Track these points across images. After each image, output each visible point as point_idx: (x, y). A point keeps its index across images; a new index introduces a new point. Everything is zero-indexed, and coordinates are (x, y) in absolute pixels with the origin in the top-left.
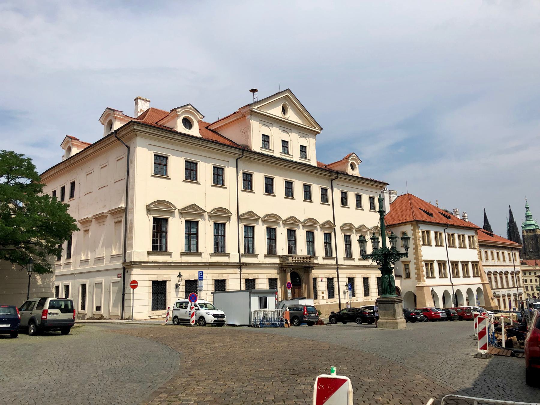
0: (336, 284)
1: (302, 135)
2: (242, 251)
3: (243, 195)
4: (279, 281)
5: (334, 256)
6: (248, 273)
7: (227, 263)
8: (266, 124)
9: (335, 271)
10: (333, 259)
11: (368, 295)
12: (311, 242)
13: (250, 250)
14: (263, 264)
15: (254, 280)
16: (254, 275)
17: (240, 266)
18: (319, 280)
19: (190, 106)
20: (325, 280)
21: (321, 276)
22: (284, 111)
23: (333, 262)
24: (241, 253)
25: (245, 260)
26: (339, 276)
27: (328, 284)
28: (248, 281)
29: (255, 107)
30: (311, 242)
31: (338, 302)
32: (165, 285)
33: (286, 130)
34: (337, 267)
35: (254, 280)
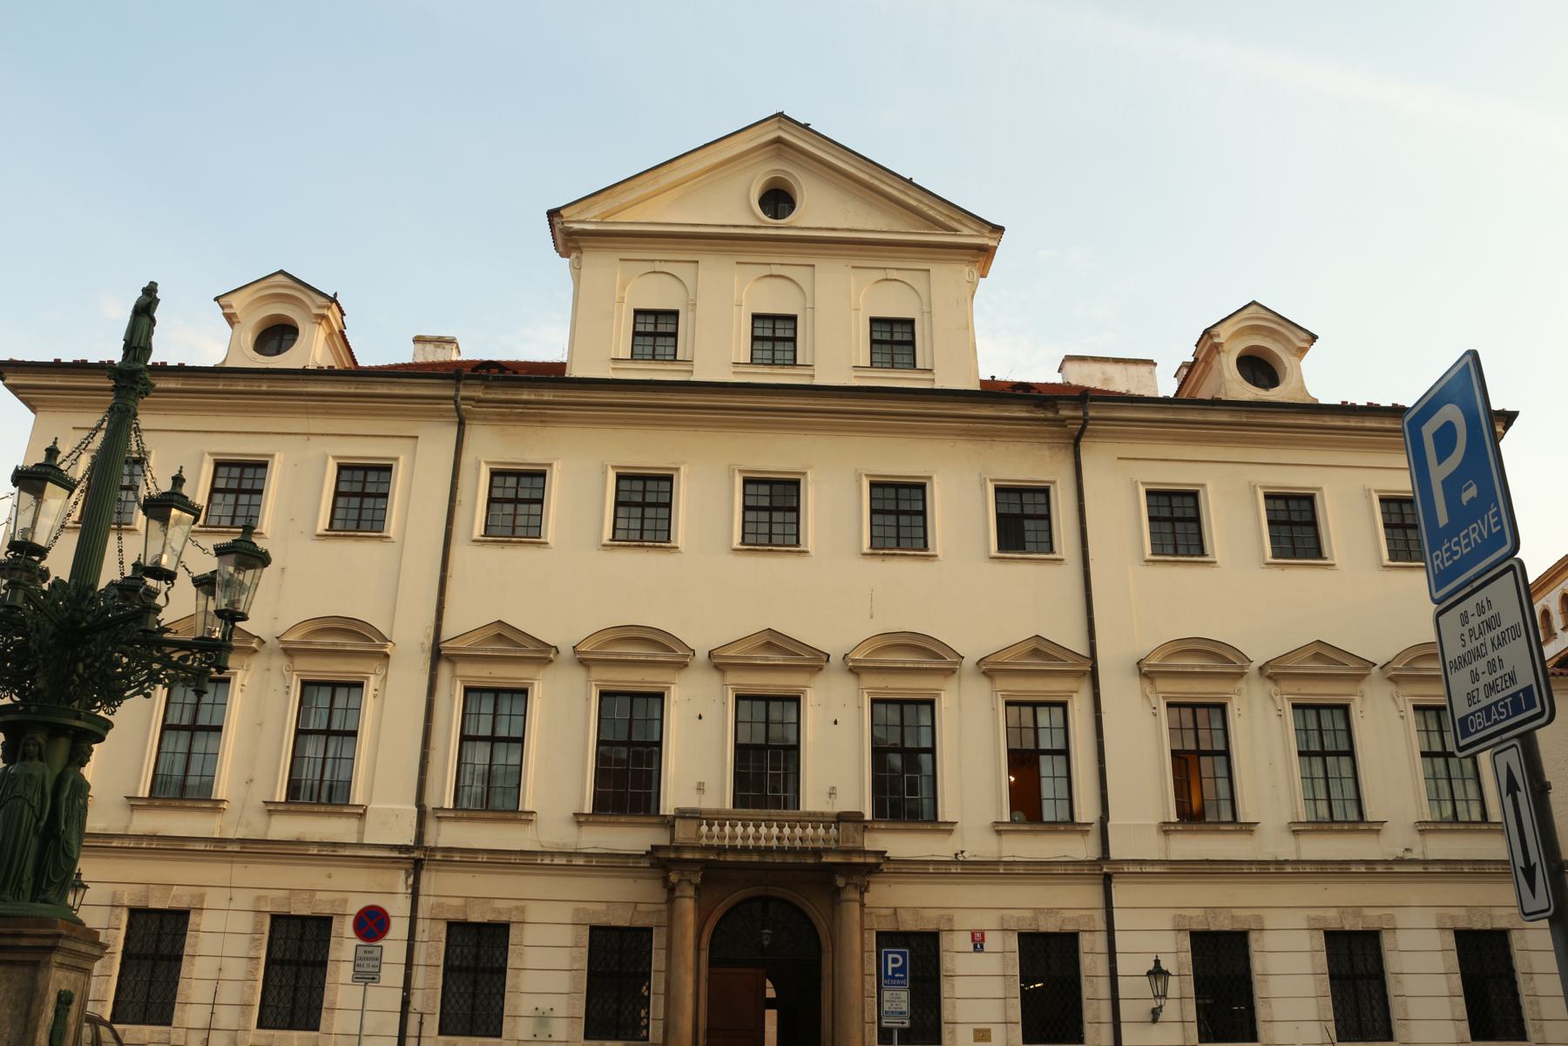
0: (1092, 962)
1: (881, 275)
2: (443, 794)
3: (472, 560)
4: (658, 941)
5: (1086, 811)
6: (451, 892)
8: (659, 267)
13: (493, 794)
14: (552, 854)
15: (505, 927)
16: (499, 904)
17: (416, 859)
19: (280, 278)
23: (1082, 849)
24: (431, 802)
25: (447, 835)
26: (1117, 925)
28: (457, 929)
33: (776, 270)
34: (1104, 872)
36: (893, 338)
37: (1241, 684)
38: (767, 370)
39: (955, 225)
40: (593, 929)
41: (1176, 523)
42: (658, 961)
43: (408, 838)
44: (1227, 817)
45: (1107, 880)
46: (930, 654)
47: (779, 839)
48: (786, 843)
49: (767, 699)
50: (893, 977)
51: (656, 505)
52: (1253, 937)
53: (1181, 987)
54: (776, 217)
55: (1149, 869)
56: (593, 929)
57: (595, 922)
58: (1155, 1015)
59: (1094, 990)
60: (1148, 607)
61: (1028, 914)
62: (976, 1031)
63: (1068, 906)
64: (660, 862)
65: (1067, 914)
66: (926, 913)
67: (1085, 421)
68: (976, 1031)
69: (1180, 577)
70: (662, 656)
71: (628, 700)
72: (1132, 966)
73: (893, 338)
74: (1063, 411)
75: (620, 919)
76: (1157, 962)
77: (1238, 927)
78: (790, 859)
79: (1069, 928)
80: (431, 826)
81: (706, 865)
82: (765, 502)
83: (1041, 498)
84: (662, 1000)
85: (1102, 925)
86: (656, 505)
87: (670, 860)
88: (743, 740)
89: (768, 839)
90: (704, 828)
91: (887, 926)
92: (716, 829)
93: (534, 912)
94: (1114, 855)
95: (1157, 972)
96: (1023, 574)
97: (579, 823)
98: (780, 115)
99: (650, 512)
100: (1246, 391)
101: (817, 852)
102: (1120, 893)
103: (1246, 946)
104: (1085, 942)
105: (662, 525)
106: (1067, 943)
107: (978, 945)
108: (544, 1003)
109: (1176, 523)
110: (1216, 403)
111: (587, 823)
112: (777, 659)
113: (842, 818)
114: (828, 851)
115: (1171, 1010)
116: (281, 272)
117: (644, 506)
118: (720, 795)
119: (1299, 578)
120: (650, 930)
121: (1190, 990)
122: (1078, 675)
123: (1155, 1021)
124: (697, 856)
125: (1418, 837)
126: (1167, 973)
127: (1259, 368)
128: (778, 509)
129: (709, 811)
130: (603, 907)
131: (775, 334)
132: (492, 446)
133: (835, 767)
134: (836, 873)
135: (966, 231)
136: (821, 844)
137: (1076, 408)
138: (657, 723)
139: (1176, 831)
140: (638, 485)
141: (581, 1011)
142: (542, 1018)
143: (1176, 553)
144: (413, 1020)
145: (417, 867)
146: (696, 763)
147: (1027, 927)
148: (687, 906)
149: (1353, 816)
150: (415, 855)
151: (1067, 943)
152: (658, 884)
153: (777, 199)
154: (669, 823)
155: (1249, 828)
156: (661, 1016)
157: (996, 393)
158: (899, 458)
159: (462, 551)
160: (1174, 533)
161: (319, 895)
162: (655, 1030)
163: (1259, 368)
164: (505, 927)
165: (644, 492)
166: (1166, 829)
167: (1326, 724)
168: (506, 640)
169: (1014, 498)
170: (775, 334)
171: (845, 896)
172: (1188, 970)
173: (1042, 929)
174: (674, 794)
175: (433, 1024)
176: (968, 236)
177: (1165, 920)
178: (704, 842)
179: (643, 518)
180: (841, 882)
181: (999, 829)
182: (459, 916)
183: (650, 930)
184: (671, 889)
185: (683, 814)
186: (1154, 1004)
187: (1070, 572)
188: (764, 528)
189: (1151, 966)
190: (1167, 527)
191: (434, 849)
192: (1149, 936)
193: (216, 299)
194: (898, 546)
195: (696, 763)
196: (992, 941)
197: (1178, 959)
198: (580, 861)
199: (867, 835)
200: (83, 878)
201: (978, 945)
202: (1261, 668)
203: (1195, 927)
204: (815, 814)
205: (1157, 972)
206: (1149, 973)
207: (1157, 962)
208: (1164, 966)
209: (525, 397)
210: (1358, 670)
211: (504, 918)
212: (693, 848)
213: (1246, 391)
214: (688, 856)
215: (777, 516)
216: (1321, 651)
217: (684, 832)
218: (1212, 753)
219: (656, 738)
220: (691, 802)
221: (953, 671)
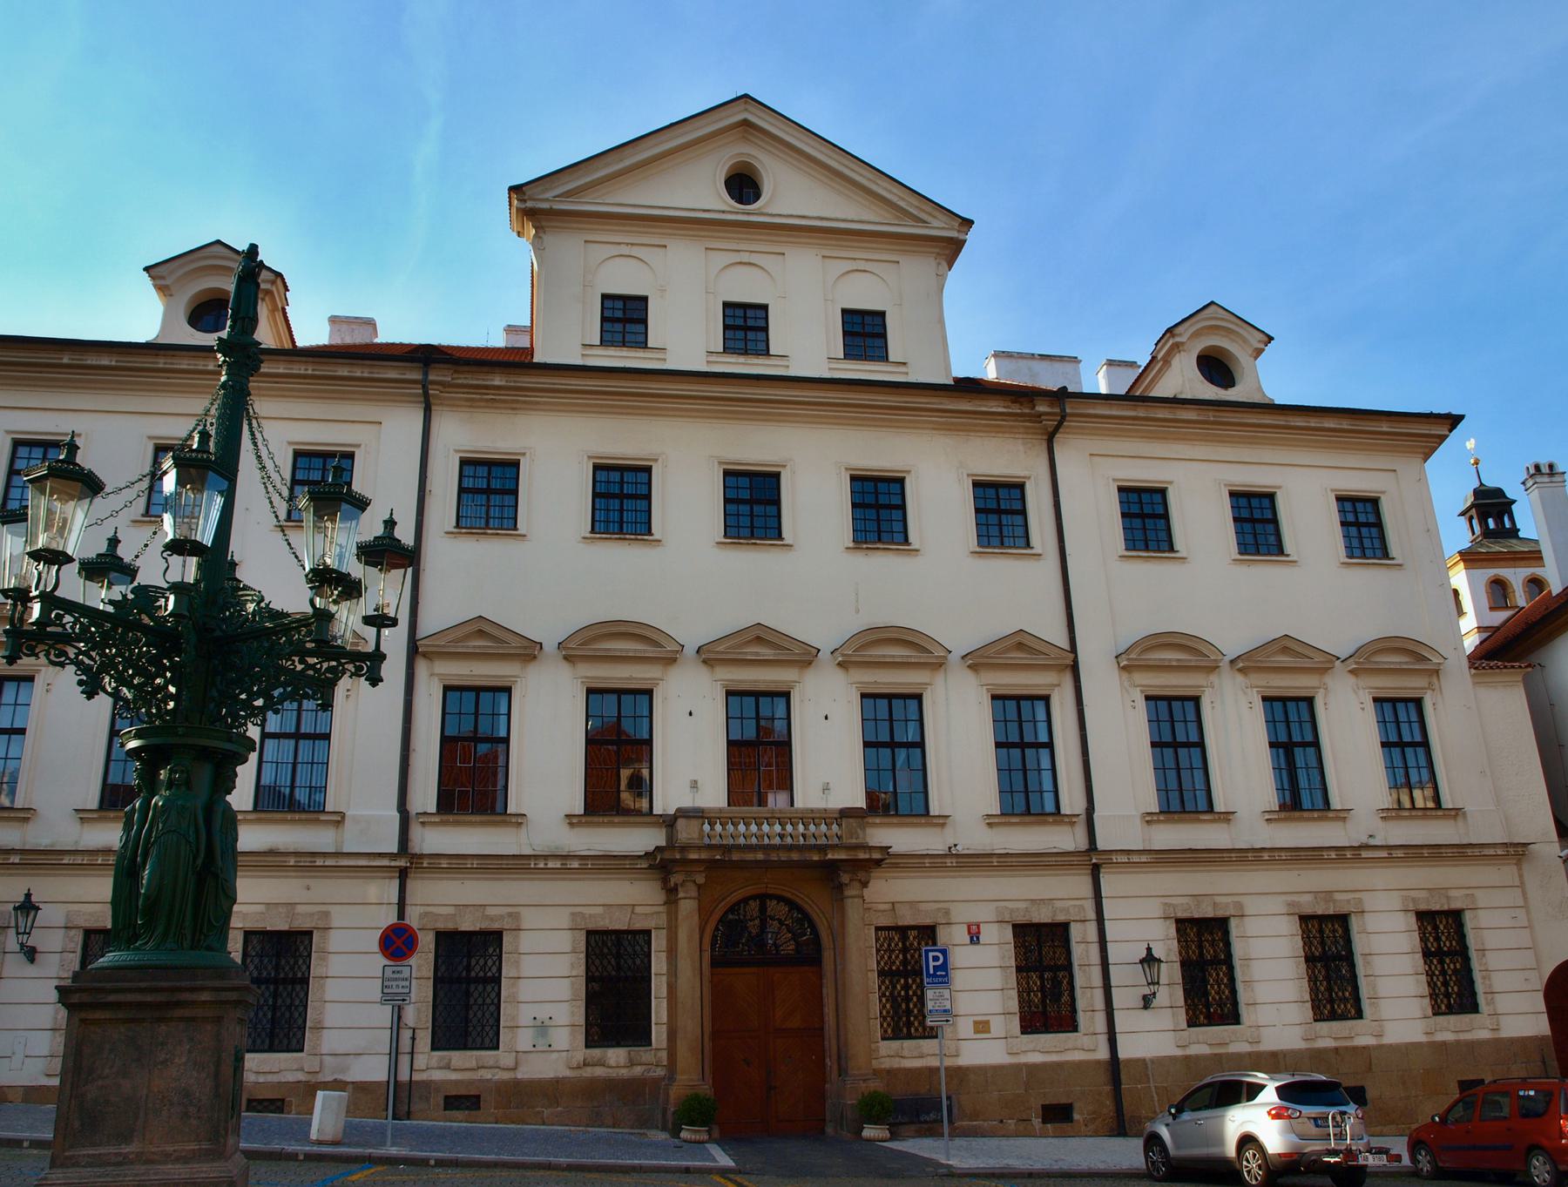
0: (1083, 951)
4: (658, 943)
5: (1072, 800)
6: (442, 902)
7: (325, 855)
8: (625, 250)
9: (1082, 884)
10: (1070, 820)
14: (546, 857)
15: (498, 935)
16: (491, 911)
21: (963, 914)
22: (743, 185)
23: (1068, 839)
25: (434, 840)
29: (549, 195)
31: (1103, 1054)
33: (745, 257)
35: (493, 939)
36: (864, 331)
37: (1213, 678)
38: (742, 359)
39: (928, 218)
40: (590, 933)
41: (1146, 519)
42: (658, 964)
44: (1202, 805)
45: (1095, 871)
46: (916, 648)
47: (782, 836)
48: (789, 840)
49: (757, 695)
50: (934, 975)
51: (635, 497)
52: (1233, 923)
53: (1170, 972)
54: (741, 202)
55: (1135, 858)
56: (590, 933)
57: (591, 926)
58: (1147, 1002)
59: (1086, 979)
60: (1122, 599)
61: (1022, 905)
62: (975, 1023)
63: (1062, 895)
64: (661, 865)
65: (1058, 904)
66: (923, 906)
67: (1063, 418)
68: (975, 1023)
69: (1149, 572)
70: (650, 651)
71: (614, 697)
72: (1125, 951)
73: (864, 331)
74: (1038, 407)
75: (619, 922)
76: (1149, 949)
77: (1220, 913)
78: (795, 856)
79: (1061, 918)
80: (416, 832)
81: (711, 865)
82: (746, 495)
83: (1016, 493)
84: (664, 1004)
85: (1092, 915)
86: (635, 497)
87: (675, 861)
88: (736, 736)
89: (782, 836)
90: (707, 827)
91: (884, 921)
92: (718, 827)
93: (529, 918)
94: (1101, 845)
95: (1149, 960)
96: (1004, 569)
97: (571, 825)
98: (746, 96)
99: (628, 504)
100: (1211, 392)
101: (822, 849)
102: (1108, 882)
103: (1226, 933)
104: (1075, 932)
105: (642, 517)
106: (1059, 932)
107: (975, 938)
108: (543, 1012)
109: (1146, 519)
110: (1175, 401)
111: (580, 824)
112: (766, 653)
113: (846, 813)
114: (834, 847)
115: (1163, 996)
117: (622, 500)
118: (714, 794)
119: (1263, 573)
120: (648, 933)
121: (1178, 977)
122: (1060, 668)
123: (1146, 1007)
124: (704, 856)
125: (1381, 824)
126: (1160, 961)
127: (1216, 367)
128: (759, 502)
129: (711, 810)
130: (600, 910)
131: (746, 325)
132: (463, 433)
133: (829, 764)
134: (837, 865)
135: (936, 223)
136: (823, 841)
137: (1051, 405)
138: (646, 721)
139: (1159, 821)
140: (615, 476)
141: (581, 1019)
142: (542, 1028)
143: (1147, 549)
144: (406, 1035)
145: (403, 874)
146: (689, 763)
147: (1021, 919)
148: (687, 906)
149: (1320, 803)
150: (402, 863)
151: (1059, 932)
152: (657, 885)
153: (743, 185)
154: (669, 822)
155: (1227, 817)
156: (665, 1020)
157: (969, 387)
158: (880, 450)
160: (1144, 529)
161: (299, 909)
162: (658, 1034)
163: (1216, 367)
164: (498, 935)
165: (622, 482)
166: (1149, 819)
167: (1402, 716)
168: (483, 636)
169: (991, 492)
170: (746, 325)
171: (848, 892)
172: (1175, 957)
173: (1036, 920)
174: (669, 794)
175: (424, 1039)
176: (939, 227)
177: (1154, 908)
178: (707, 841)
179: (621, 511)
180: (845, 878)
181: (991, 822)
182: (450, 926)
183: (648, 933)
184: (671, 893)
185: (683, 813)
186: (1147, 991)
187: (1049, 566)
188: (745, 521)
189: (1144, 954)
190: (1137, 523)
191: (422, 856)
192: (1139, 922)
193: (147, 269)
194: (880, 540)
195: (689, 763)
196: (989, 933)
197: (1166, 946)
198: (575, 864)
199: (869, 831)
200: (33, 899)
201: (975, 938)
202: (1232, 662)
203: (1181, 915)
204: (819, 811)
205: (1149, 960)
206: (1142, 962)
207: (1149, 949)
208: (1156, 954)
209: (497, 383)
210: (1323, 663)
211: (496, 926)
212: (699, 848)
213: (1211, 392)
214: (693, 856)
215: (758, 509)
216: (1286, 645)
217: (687, 832)
218: (1304, 745)
219: (646, 736)
220: (687, 801)
221: (941, 665)
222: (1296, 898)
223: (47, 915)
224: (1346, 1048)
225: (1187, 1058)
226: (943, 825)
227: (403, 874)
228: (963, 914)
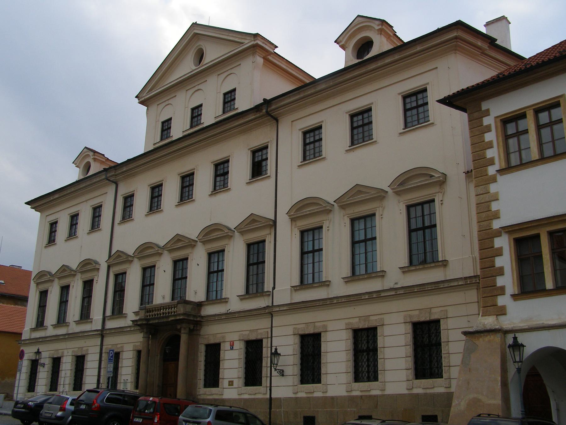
11: (318, 380)
12: (215, 272)
18: (225, 346)
20: (240, 346)
21: (229, 337)
27: (247, 353)
30: (215, 272)
32: (59, 362)
43: (100, 328)
61: (247, 333)
65: (260, 331)
79: (259, 337)
107: (232, 348)
116: (359, 16)
126: (280, 354)
145: (103, 337)
147: (247, 338)
159: (116, 227)
161: (84, 349)
196: (237, 345)
201: (232, 348)
208: (279, 352)
222: (351, 321)
223: (44, 355)
224: (366, 396)
225: (296, 398)
226: (227, 302)
227: (103, 337)
228: (229, 337)
